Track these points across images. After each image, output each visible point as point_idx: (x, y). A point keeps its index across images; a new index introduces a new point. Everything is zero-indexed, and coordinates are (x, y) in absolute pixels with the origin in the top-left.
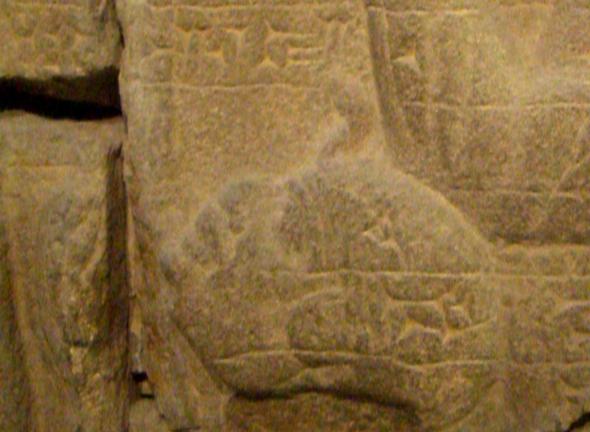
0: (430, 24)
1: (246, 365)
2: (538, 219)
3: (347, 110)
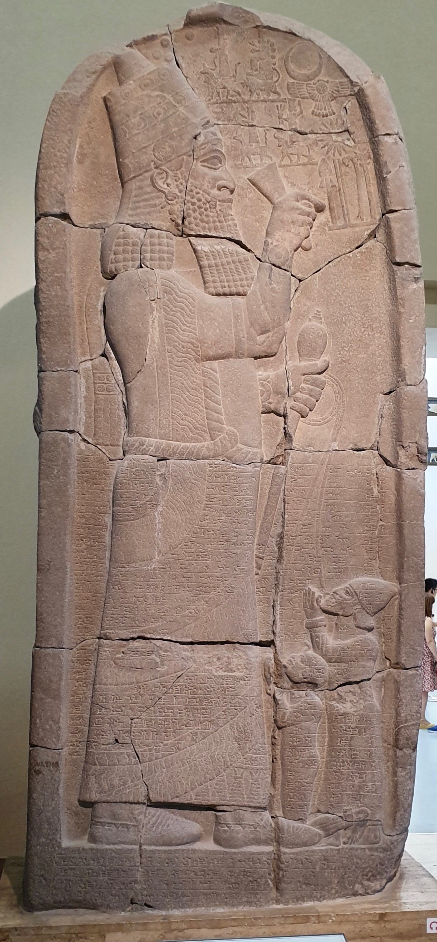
0: (320, 635)
1: (296, 679)
2: (333, 661)
3: (307, 645)
